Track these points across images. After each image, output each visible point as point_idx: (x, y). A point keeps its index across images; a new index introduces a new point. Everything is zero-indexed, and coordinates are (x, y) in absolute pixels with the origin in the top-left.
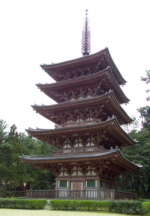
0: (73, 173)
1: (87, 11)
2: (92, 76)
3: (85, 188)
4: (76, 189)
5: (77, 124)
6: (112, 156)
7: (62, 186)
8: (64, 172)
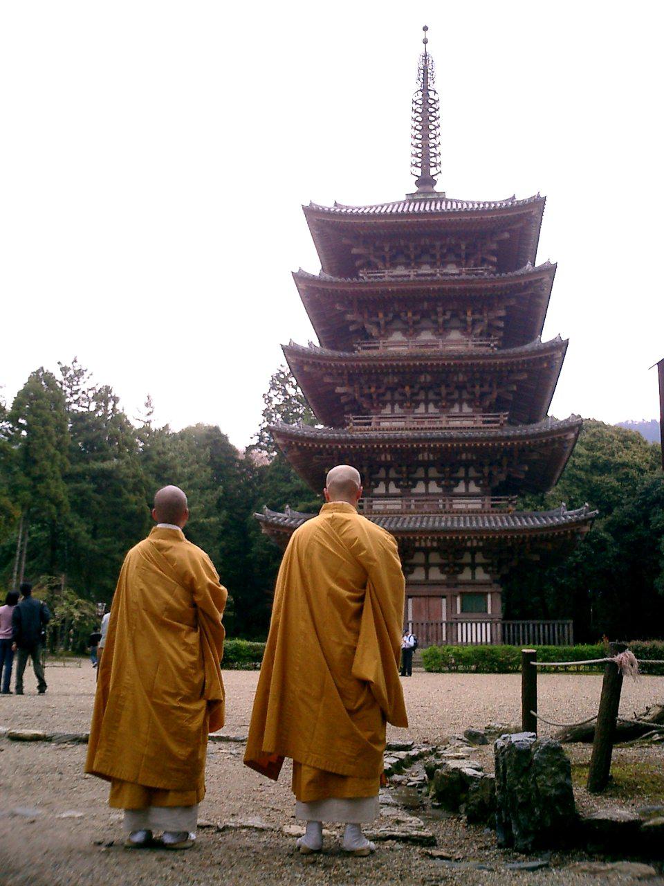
1: (425, 29)
3: (454, 616)
4: (423, 619)
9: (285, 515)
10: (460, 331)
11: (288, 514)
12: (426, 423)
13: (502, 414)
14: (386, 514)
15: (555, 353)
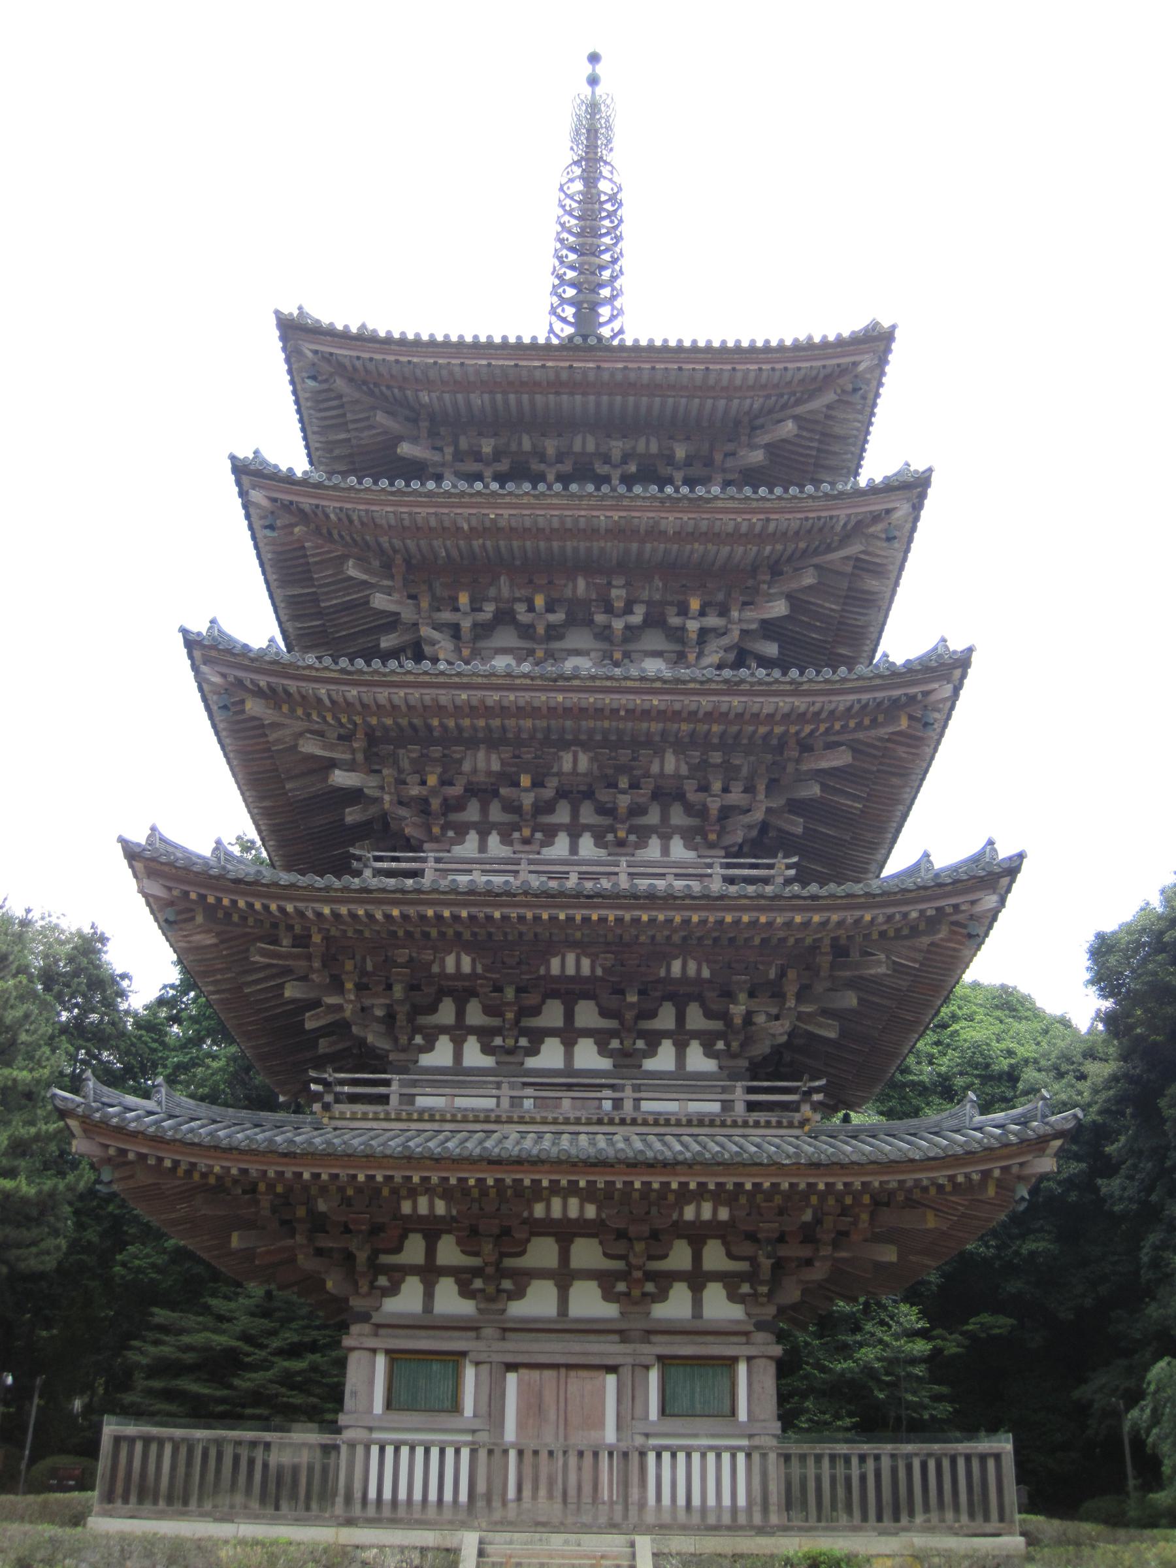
0: (519, 1293)
1: (594, 58)
2: (783, 504)
4: (549, 1438)
6: (990, 1171)
7: (411, 1407)
9: (150, 1104)
10: (666, 661)
11: (159, 1103)
13: (781, 862)
14: (454, 1120)
15: (936, 686)
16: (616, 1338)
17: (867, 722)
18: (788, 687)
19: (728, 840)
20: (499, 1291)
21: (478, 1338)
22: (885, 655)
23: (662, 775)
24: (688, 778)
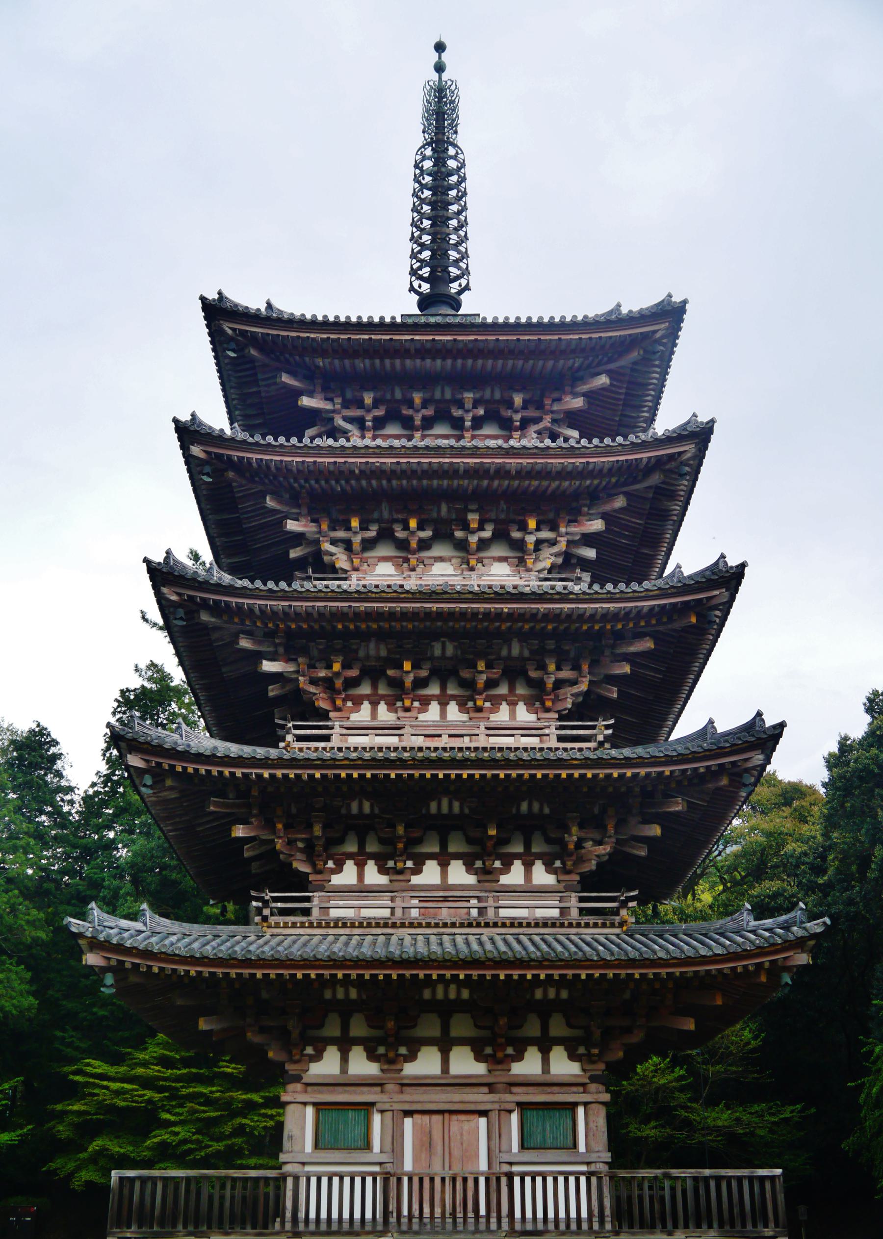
0: (412, 1057)
1: (440, 47)
3: (506, 1158)
5: (445, 738)
8: (550, 1049)
9: (138, 925)
12: (445, 738)
14: (361, 925)
16: (485, 1089)
17: (665, 620)
18: (605, 596)
19: (560, 706)
20: (398, 1055)
21: (382, 1092)
22: (678, 567)
23: (509, 657)
24: (529, 659)
